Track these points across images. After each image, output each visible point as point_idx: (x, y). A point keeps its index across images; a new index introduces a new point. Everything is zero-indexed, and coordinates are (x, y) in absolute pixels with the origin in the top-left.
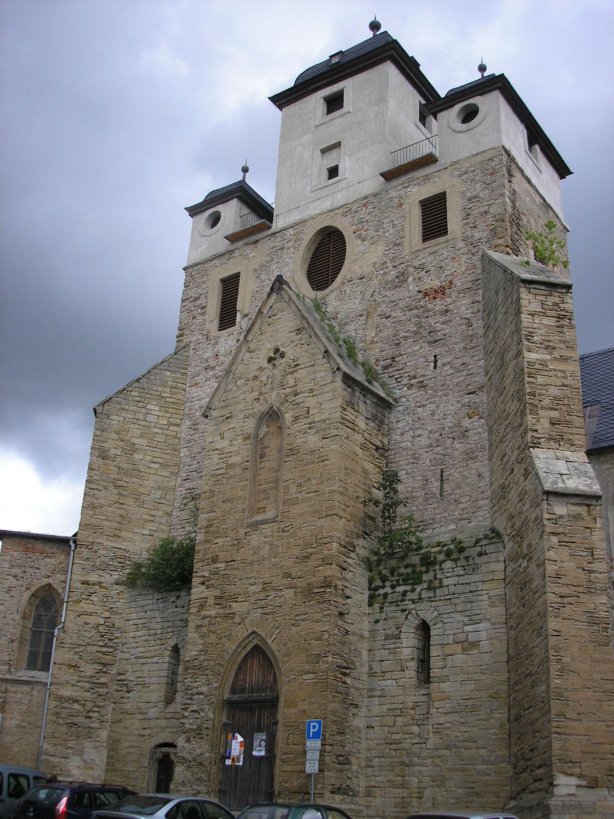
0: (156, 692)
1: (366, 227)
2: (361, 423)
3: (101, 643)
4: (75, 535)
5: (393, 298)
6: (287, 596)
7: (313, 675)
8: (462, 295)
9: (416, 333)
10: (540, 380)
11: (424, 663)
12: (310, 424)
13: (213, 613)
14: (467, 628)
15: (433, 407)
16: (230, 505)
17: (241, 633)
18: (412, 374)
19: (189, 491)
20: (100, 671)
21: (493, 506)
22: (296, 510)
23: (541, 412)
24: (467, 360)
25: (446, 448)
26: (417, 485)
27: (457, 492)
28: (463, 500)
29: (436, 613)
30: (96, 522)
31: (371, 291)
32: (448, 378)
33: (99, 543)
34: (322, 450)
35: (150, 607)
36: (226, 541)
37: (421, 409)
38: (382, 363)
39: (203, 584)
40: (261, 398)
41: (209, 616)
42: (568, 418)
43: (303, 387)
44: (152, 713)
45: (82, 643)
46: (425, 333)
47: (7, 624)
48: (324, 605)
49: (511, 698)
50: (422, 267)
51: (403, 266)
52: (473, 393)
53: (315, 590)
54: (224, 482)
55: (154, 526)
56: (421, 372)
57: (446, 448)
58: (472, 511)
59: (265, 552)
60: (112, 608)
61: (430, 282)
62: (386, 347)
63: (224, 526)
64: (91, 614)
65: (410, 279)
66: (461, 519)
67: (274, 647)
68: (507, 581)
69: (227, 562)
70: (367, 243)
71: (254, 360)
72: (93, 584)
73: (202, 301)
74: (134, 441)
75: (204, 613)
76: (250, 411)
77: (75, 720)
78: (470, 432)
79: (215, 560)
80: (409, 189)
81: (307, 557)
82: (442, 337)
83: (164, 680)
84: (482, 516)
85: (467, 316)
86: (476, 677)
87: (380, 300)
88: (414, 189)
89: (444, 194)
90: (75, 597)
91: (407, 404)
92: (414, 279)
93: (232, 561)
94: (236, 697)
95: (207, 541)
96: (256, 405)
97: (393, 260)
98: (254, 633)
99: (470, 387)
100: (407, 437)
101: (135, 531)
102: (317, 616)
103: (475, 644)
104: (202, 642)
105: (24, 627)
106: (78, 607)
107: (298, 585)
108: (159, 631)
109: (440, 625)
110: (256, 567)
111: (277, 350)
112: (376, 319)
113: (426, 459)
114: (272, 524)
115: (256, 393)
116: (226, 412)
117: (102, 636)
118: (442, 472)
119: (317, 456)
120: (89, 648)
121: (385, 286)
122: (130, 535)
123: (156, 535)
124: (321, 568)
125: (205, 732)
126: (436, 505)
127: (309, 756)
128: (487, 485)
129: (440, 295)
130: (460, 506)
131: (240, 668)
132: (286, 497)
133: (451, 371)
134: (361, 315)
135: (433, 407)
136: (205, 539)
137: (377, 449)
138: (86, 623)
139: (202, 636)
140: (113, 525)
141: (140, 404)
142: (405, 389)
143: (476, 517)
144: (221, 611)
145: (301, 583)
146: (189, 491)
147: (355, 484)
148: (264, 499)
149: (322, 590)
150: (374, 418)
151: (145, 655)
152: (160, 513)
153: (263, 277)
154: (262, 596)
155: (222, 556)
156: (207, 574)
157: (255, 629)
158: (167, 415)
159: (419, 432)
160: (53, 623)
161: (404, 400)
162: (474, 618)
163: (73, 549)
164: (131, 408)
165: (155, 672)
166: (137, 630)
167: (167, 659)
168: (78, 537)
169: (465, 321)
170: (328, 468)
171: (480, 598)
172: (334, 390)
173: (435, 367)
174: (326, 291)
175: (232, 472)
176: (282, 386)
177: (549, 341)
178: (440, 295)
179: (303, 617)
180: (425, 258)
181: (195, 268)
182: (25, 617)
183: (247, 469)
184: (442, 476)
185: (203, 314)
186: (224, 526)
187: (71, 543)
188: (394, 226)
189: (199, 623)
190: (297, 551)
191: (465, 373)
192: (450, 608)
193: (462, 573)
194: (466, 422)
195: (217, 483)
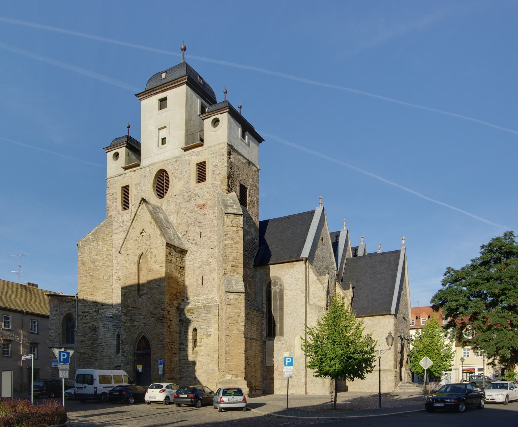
0: (113, 349)
2: (174, 260)
11: (195, 341)
13: (129, 325)
14: (208, 330)
20: (93, 343)
44: (113, 356)
50: (197, 194)
55: (106, 290)
59: (144, 305)
61: (200, 202)
64: (87, 323)
65: (193, 199)
73: (115, 196)
74: (94, 257)
77: (86, 360)
79: (128, 307)
80: (193, 157)
81: (157, 308)
83: (116, 345)
88: (194, 157)
89: (205, 162)
90: (80, 317)
94: (138, 352)
95: (125, 300)
96: (137, 251)
100: (191, 263)
105: (63, 328)
113: (197, 272)
116: (127, 252)
122: (98, 294)
127: (162, 369)
129: (202, 208)
137: (181, 268)
139: (126, 332)
140: (90, 290)
152: (108, 285)
153: (139, 189)
158: (106, 246)
159: (195, 262)
160: (73, 327)
164: (92, 243)
165: (113, 342)
166: (104, 328)
172: (163, 249)
180: (197, 190)
182: (63, 325)
185: (116, 202)
194: (210, 260)
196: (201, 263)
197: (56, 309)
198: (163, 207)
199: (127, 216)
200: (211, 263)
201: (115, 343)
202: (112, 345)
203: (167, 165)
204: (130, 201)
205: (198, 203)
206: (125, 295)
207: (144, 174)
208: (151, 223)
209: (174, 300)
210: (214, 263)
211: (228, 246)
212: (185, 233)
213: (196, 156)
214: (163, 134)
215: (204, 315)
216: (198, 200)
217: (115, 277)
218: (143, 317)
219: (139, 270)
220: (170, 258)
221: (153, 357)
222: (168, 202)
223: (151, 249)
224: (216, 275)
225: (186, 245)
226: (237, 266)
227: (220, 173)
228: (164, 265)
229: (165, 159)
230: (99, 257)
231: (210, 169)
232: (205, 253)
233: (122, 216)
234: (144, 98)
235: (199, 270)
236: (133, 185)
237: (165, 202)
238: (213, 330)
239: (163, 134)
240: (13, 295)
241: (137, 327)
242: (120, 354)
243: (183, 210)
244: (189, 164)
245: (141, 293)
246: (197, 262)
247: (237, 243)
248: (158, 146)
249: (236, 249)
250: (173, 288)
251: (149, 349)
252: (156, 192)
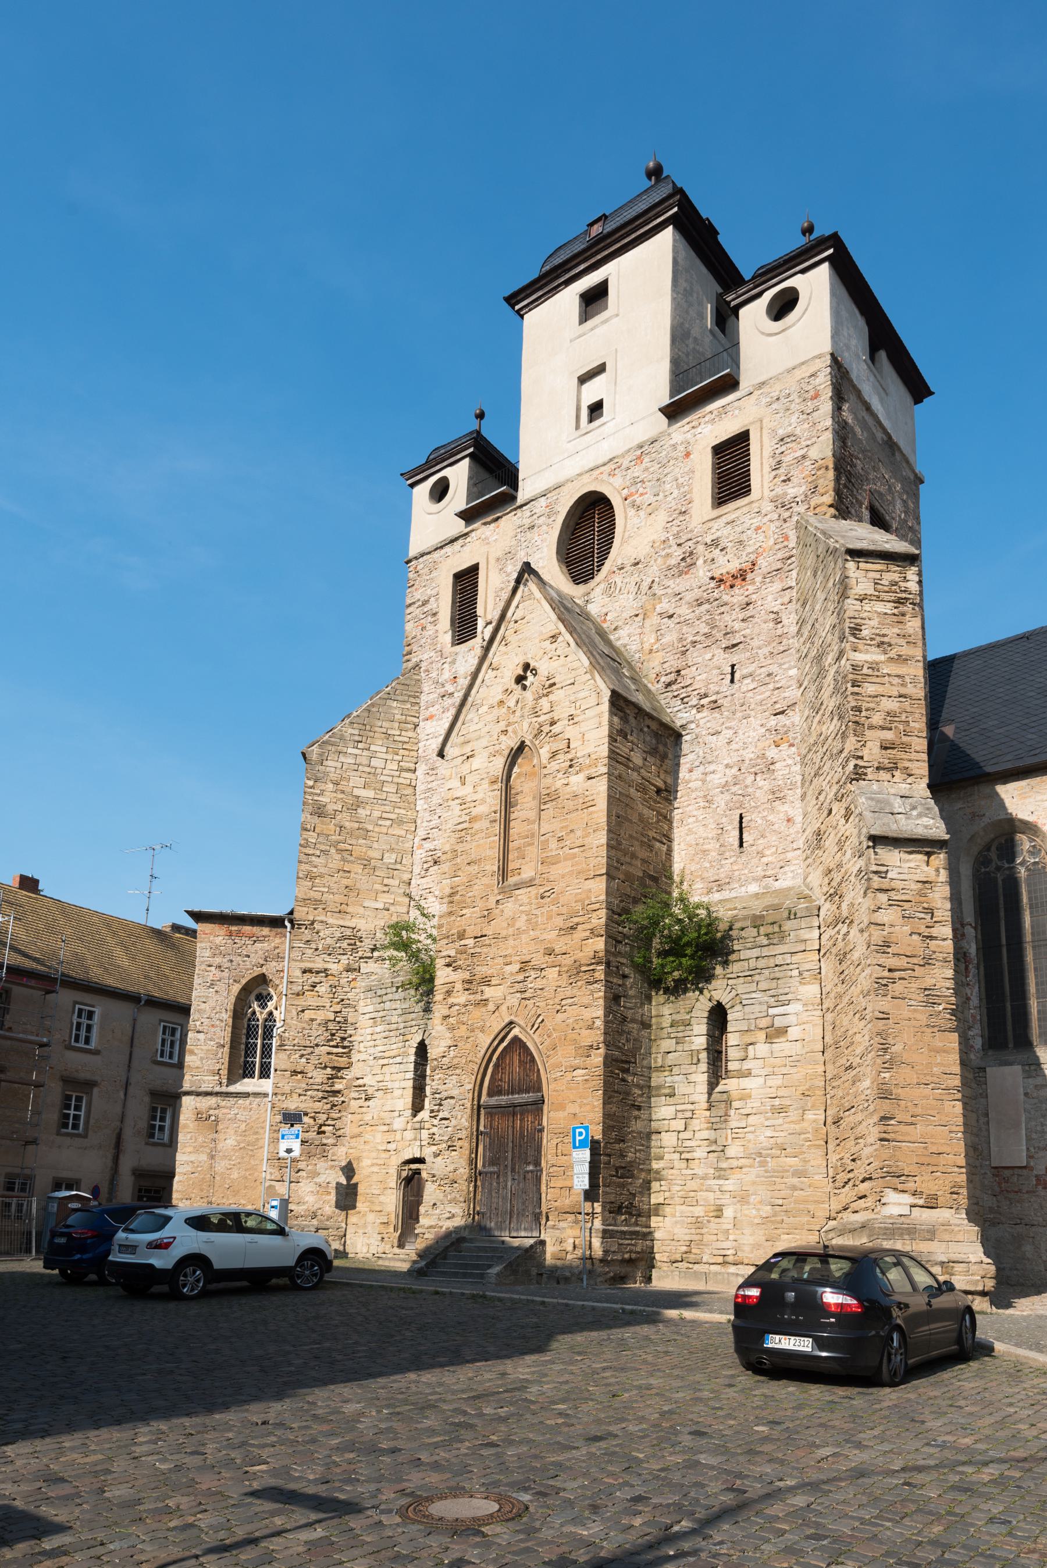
1: (641, 490)
2: (637, 759)
3: (332, 1043)
4: (291, 913)
5: (677, 590)
6: (550, 976)
8: (768, 580)
9: (707, 635)
10: (870, 689)
12: (571, 760)
15: (728, 734)
16: (476, 867)
17: (496, 1025)
18: (703, 691)
19: (431, 853)
20: (332, 1077)
21: (807, 858)
22: (556, 871)
23: (867, 732)
24: (774, 669)
25: (746, 787)
26: (710, 836)
27: (760, 842)
28: (767, 852)
29: (734, 993)
30: (317, 895)
31: (650, 580)
32: (750, 694)
33: (322, 922)
34: (587, 793)
35: (390, 996)
36: (474, 912)
37: (715, 737)
38: (663, 679)
39: (448, 965)
40: (510, 729)
41: (458, 1005)
42: (905, 739)
43: (561, 713)
45: (308, 1043)
46: (719, 635)
47: (213, 1026)
48: (595, 985)
49: (828, 1096)
51: (690, 543)
52: (782, 712)
53: (584, 968)
54: (469, 839)
55: (388, 898)
56: (713, 688)
57: (746, 787)
58: (779, 866)
59: (521, 923)
60: (343, 1000)
62: (670, 657)
63: (470, 894)
64: (318, 1008)
65: (700, 562)
66: (765, 877)
67: (535, 1037)
68: (822, 953)
69: (476, 938)
70: (642, 513)
71: (498, 680)
72: (318, 972)
75: (451, 1000)
76: (497, 747)
78: (777, 765)
79: (461, 936)
82: (742, 639)
84: (792, 871)
85: (775, 610)
86: (785, 1071)
87: (662, 592)
90: (297, 988)
91: (697, 731)
92: (705, 562)
93: (482, 936)
94: (494, 1101)
95: (450, 913)
96: (503, 738)
97: (677, 536)
98: (511, 1023)
99: (777, 706)
100: (697, 773)
101: (365, 905)
102: (586, 1000)
103: (783, 1031)
104: (451, 1036)
106: (301, 1002)
107: (564, 962)
108: (402, 1025)
109: (738, 1007)
110: (511, 942)
111: (527, 667)
112: (655, 619)
113: (721, 801)
114: (529, 889)
115: (502, 725)
116: (467, 750)
117: (333, 1035)
118: (741, 817)
119: (581, 801)
120: (317, 1050)
121: (668, 572)
122: (361, 910)
123: (392, 908)
124: (590, 941)
125: (459, 1144)
126: (734, 859)
128: (798, 832)
129: (738, 581)
130: (765, 860)
131: (497, 1066)
132: (545, 855)
133: (751, 687)
134: (637, 615)
135: (728, 734)
136: (450, 909)
137: (659, 791)
138: (312, 1020)
139: (452, 1029)
140: (339, 898)
141: (360, 745)
142: (694, 711)
143: (785, 873)
144: (472, 997)
145: (567, 961)
146: (431, 853)
147: (631, 836)
148: (518, 858)
149: (591, 967)
150: (653, 752)
151: (386, 1054)
154: (520, 977)
155: (471, 931)
156: (452, 953)
157: (512, 1018)
159: (711, 768)
161: (693, 726)
162: (781, 998)
163: (289, 929)
167: (412, 1058)
168: (296, 915)
169: (773, 616)
170: (595, 816)
171: (789, 973)
172: (600, 716)
173: (732, 681)
174: (592, 583)
175: (477, 826)
176: (536, 714)
177: (884, 635)
178: (738, 581)
179: (570, 1001)
181: (421, 560)
183: (495, 821)
184: (741, 822)
186: (470, 894)
187: (287, 923)
188: (678, 487)
189: (446, 1012)
190: (559, 922)
191: (771, 686)
192: (753, 987)
193: (765, 942)
194: (772, 753)
195: (461, 840)
196: (734, 770)
197: (218, 960)
198: (593, 609)
199: (469, 654)
200: (778, 766)
201: (411, 1075)
202: (397, 1085)
203: (605, 477)
204: (480, 611)
205: (717, 575)
206: (451, 895)
207: (527, 522)
208: (554, 638)
209: (636, 901)
210: (788, 764)
211: (865, 671)
212: (672, 677)
213: (714, 424)
214: (592, 392)
215: (756, 952)
216: (721, 560)
217: (420, 854)
218: (517, 967)
219: (508, 803)
220: (624, 749)
221: (552, 1118)
222: (610, 590)
223: (553, 723)
224: (798, 804)
225: (678, 715)
226: (905, 747)
227: (804, 457)
228: (605, 770)
229: (600, 462)
230: (371, 794)
231: (767, 452)
232: (751, 734)
233: (453, 662)
234: (530, 307)
235: (727, 796)
236: (492, 561)
237: (598, 590)
238: (802, 1015)
239: (592, 392)
240: (118, 952)
241: (491, 1007)
242: (424, 1115)
243: (664, 606)
244: (688, 455)
245: (512, 880)
246: (720, 768)
247: (901, 660)
248: (577, 427)
249: (896, 681)
250: (634, 856)
251: (540, 1089)
252: (565, 570)
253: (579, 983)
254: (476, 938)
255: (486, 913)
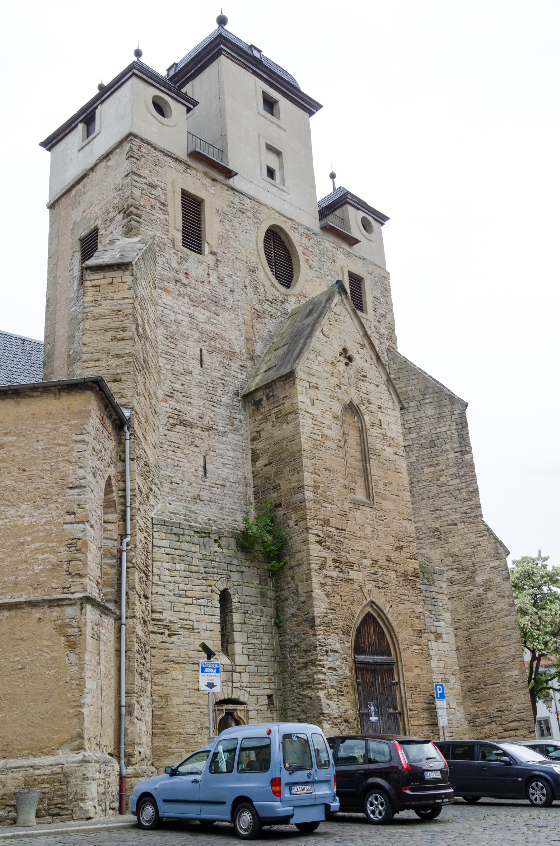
7: (420, 647)
93: (342, 530)
107: (399, 569)
114: (370, 509)
139: (328, 596)
144: (341, 575)
145: (401, 570)
253: (409, 587)
254: (337, 529)
255: (344, 513)
